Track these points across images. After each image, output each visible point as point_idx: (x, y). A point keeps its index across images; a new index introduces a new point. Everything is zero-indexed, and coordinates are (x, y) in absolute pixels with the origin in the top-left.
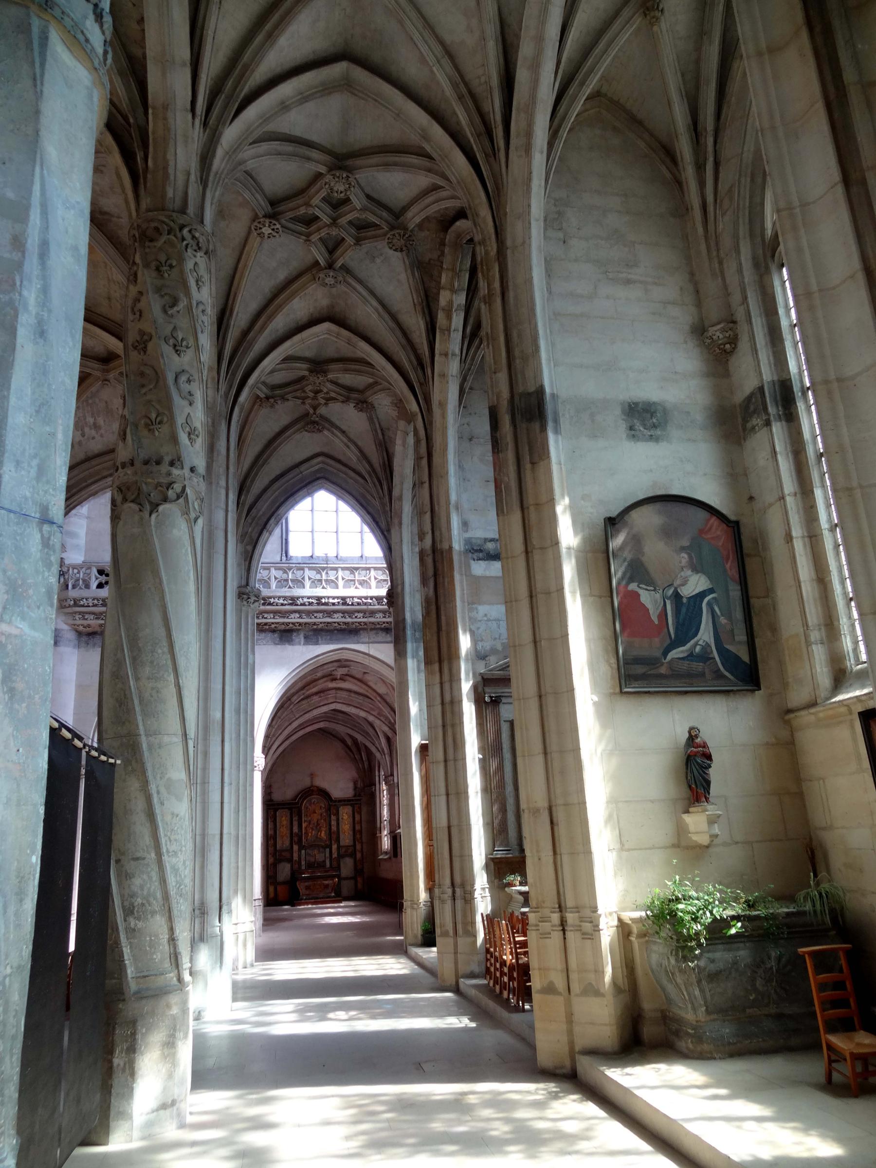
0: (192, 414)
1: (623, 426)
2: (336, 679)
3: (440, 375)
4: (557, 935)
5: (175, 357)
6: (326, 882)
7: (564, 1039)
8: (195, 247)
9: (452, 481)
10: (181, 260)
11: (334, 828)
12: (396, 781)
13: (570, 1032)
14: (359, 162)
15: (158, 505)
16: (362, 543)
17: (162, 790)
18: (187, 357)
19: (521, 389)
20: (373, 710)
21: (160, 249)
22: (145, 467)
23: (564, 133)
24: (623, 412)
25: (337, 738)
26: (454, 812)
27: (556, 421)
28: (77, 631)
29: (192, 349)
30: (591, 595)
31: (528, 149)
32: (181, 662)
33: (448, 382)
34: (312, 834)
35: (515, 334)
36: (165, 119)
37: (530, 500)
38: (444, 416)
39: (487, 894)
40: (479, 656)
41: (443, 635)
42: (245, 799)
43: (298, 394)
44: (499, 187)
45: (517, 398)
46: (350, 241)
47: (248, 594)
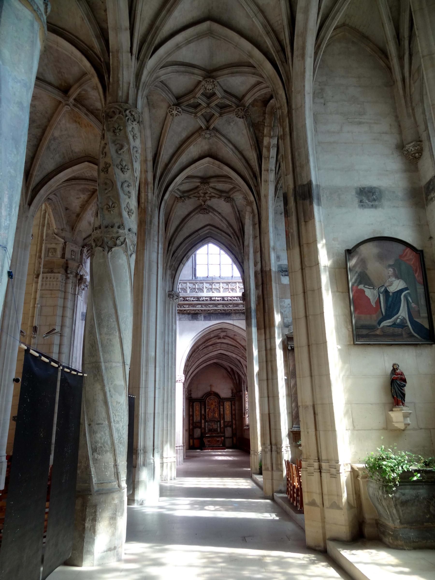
0: (130, 203)
1: (356, 201)
2: (220, 338)
3: (264, 181)
4: (317, 474)
5: (121, 174)
6: (218, 439)
7: (321, 531)
8: (132, 119)
9: (271, 235)
10: (125, 126)
11: (222, 412)
13: (324, 528)
14: (219, 73)
15: (112, 248)
16: (232, 270)
17: (112, 390)
18: (128, 174)
19: (299, 183)
21: (115, 121)
22: (106, 229)
23: (323, 46)
24: (357, 193)
25: (223, 367)
26: (271, 406)
27: (319, 199)
29: (130, 170)
30: (338, 291)
31: (303, 56)
32: (122, 326)
33: (268, 185)
34: (211, 415)
35: (296, 154)
36: (118, 57)
37: (304, 241)
38: (267, 202)
39: (289, 449)
40: (285, 325)
41: (267, 314)
42: (171, 396)
43: (196, 195)
44: (289, 79)
45: (297, 188)
46: (217, 115)
47: (173, 295)
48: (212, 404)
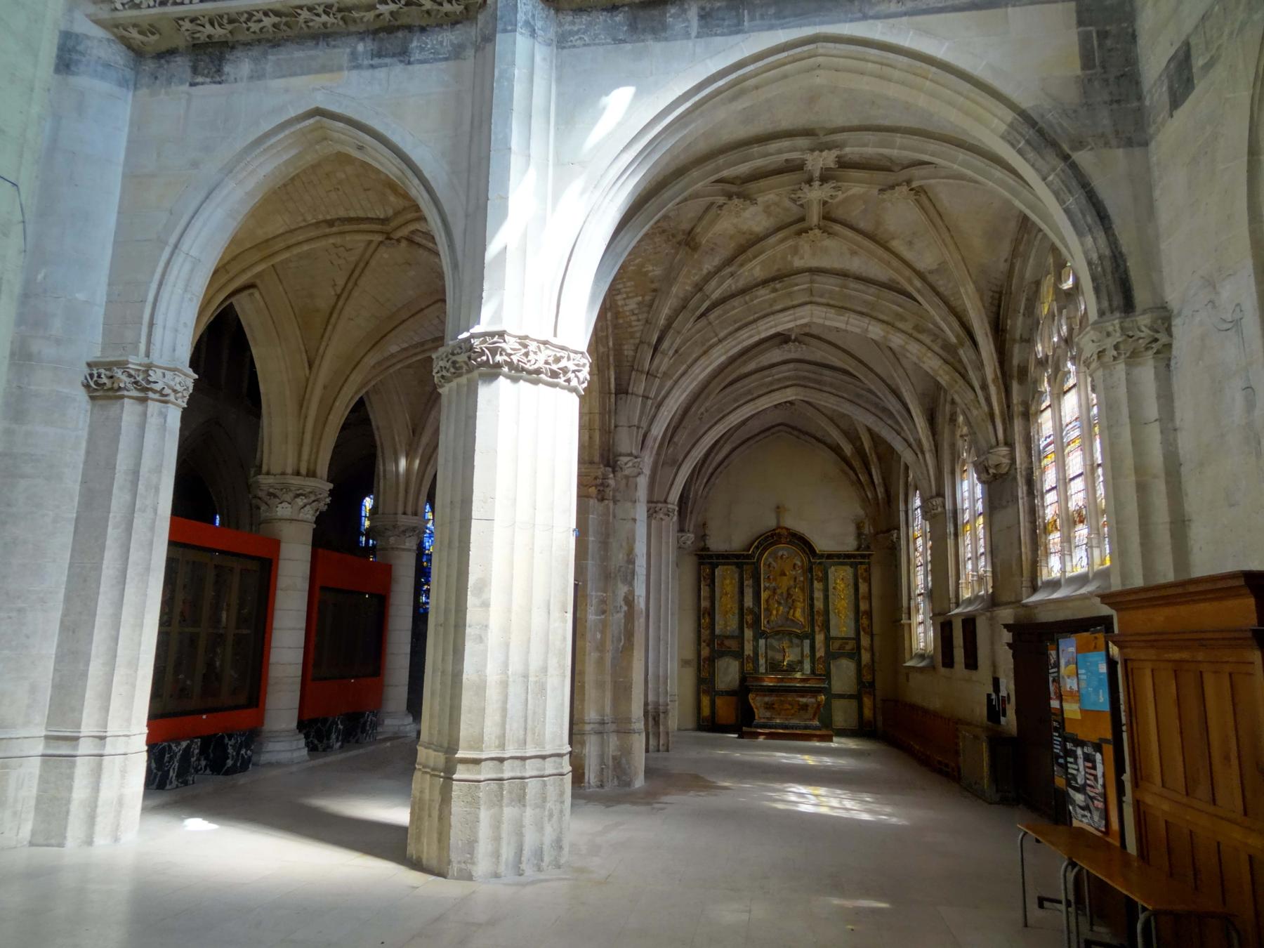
6: (804, 700)
11: (819, 605)
12: (949, 506)
20: (902, 319)
25: (825, 443)
28: (130, 47)
34: (778, 611)
48: (783, 574)
